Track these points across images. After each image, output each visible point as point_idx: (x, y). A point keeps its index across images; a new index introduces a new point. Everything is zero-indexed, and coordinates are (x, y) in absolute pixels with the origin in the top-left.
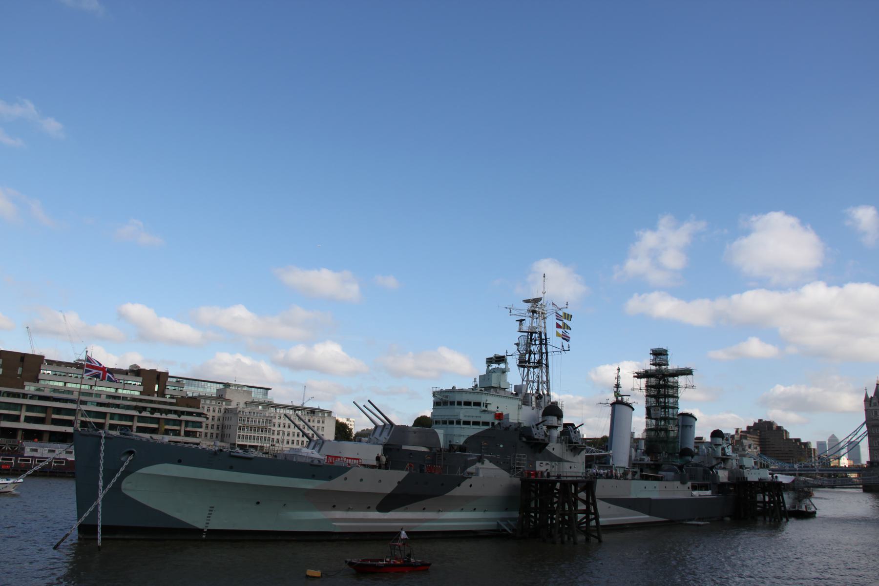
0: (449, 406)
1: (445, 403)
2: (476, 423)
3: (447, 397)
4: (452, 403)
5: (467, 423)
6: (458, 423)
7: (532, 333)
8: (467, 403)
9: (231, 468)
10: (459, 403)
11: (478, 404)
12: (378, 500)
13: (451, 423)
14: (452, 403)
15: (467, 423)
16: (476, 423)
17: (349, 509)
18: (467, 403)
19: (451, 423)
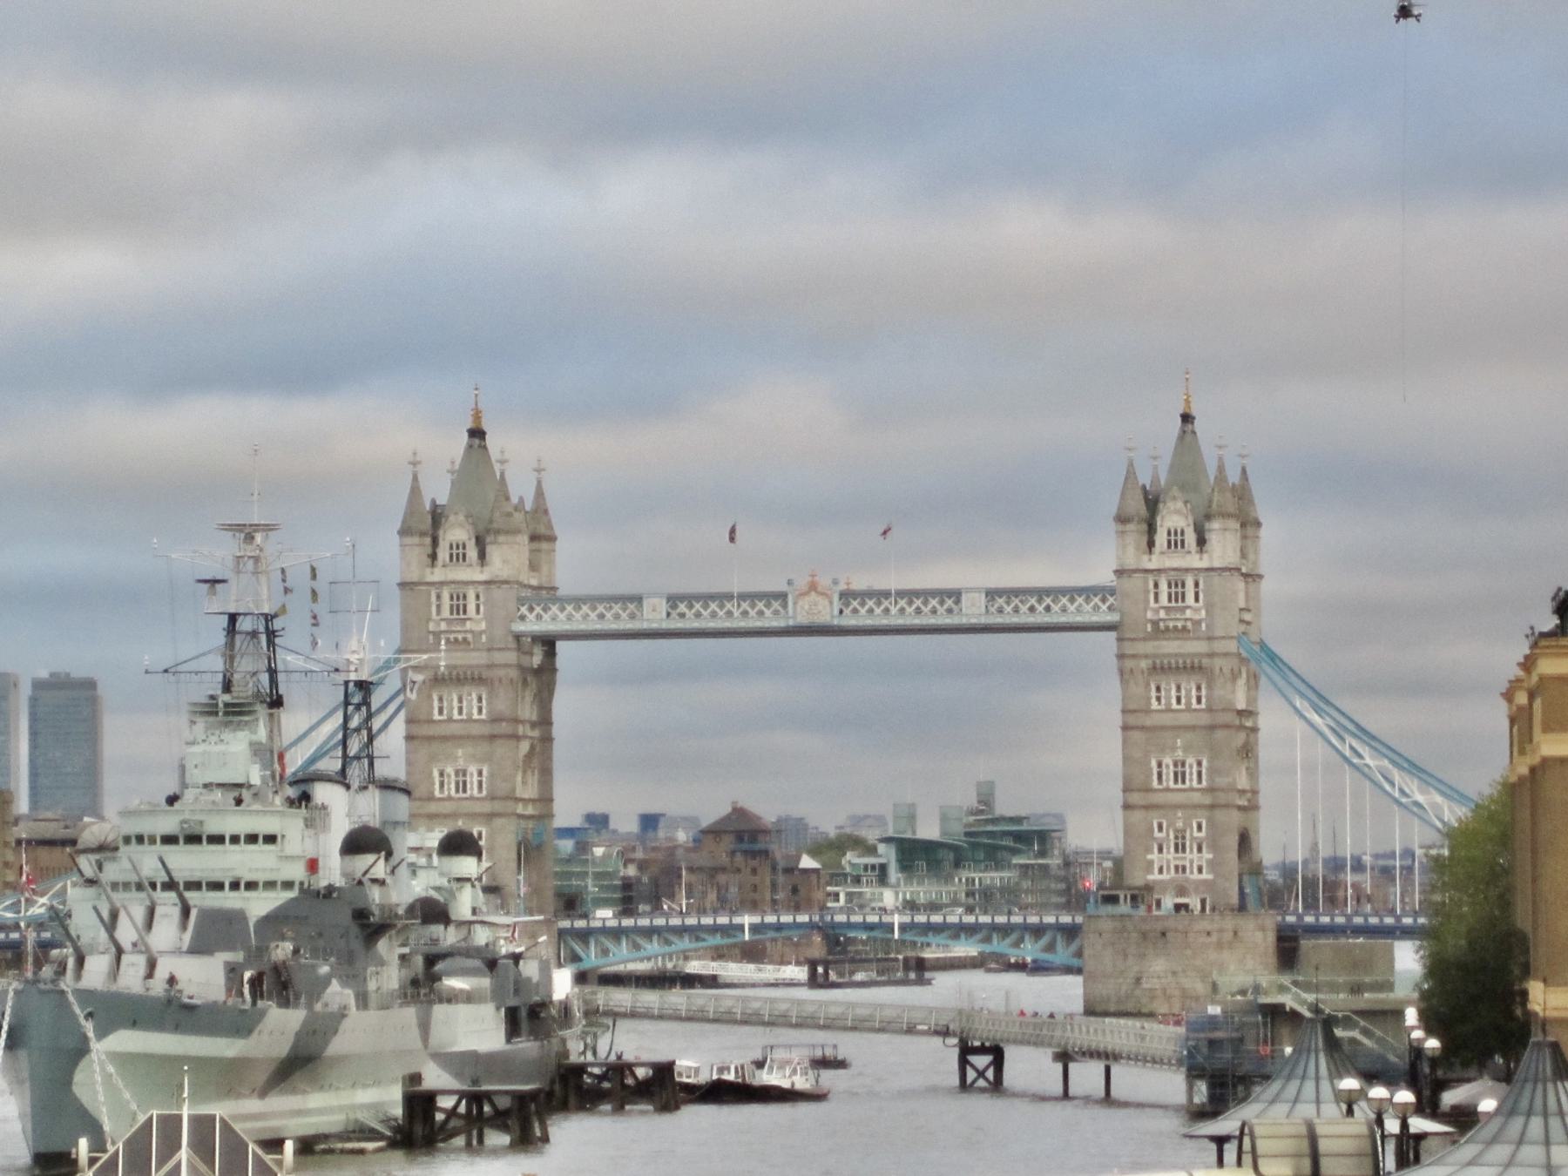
0: (205, 846)
1: (193, 839)
2: (270, 885)
3: (201, 823)
4: (217, 839)
5: (251, 886)
6: (235, 886)
7: (233, 618)
8: (252, 839)
9: (177, 1028)
10: (235, 839)
11: (271, 839)
12: (261, 1077)
13: (217, 886)
14: (217, 839)
15: (251, 886)
16: (270, 885)
17: (239, 1096)
18: (252, 839)
19: (217, 886)
